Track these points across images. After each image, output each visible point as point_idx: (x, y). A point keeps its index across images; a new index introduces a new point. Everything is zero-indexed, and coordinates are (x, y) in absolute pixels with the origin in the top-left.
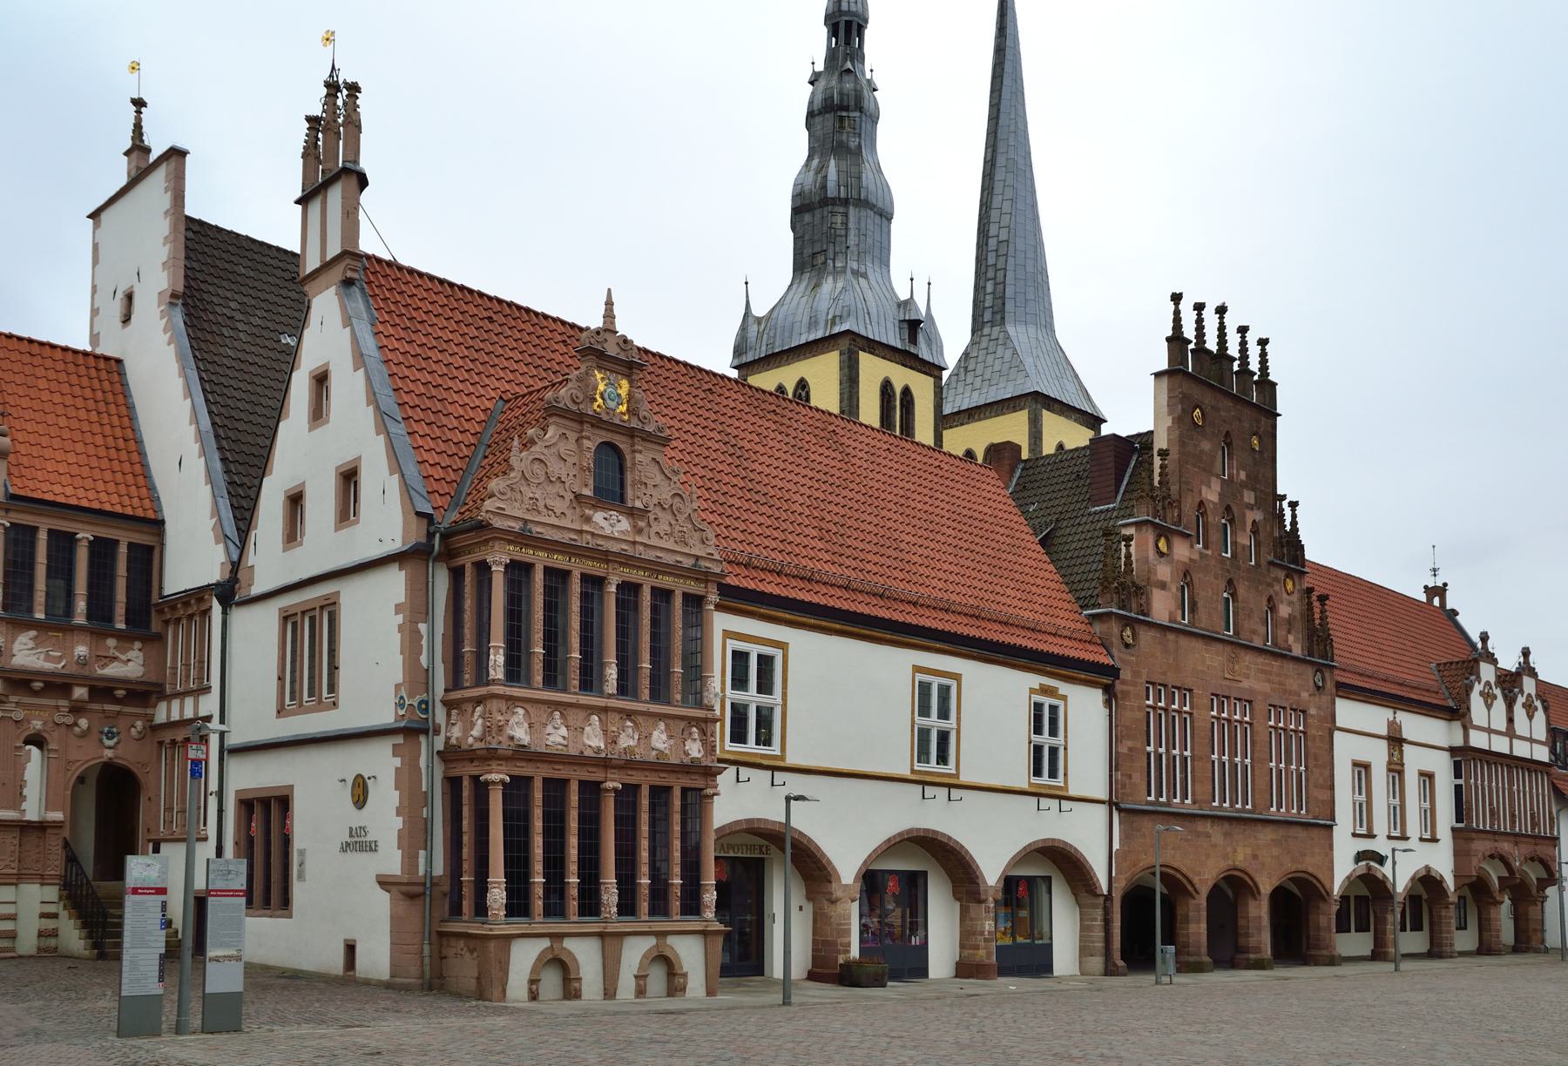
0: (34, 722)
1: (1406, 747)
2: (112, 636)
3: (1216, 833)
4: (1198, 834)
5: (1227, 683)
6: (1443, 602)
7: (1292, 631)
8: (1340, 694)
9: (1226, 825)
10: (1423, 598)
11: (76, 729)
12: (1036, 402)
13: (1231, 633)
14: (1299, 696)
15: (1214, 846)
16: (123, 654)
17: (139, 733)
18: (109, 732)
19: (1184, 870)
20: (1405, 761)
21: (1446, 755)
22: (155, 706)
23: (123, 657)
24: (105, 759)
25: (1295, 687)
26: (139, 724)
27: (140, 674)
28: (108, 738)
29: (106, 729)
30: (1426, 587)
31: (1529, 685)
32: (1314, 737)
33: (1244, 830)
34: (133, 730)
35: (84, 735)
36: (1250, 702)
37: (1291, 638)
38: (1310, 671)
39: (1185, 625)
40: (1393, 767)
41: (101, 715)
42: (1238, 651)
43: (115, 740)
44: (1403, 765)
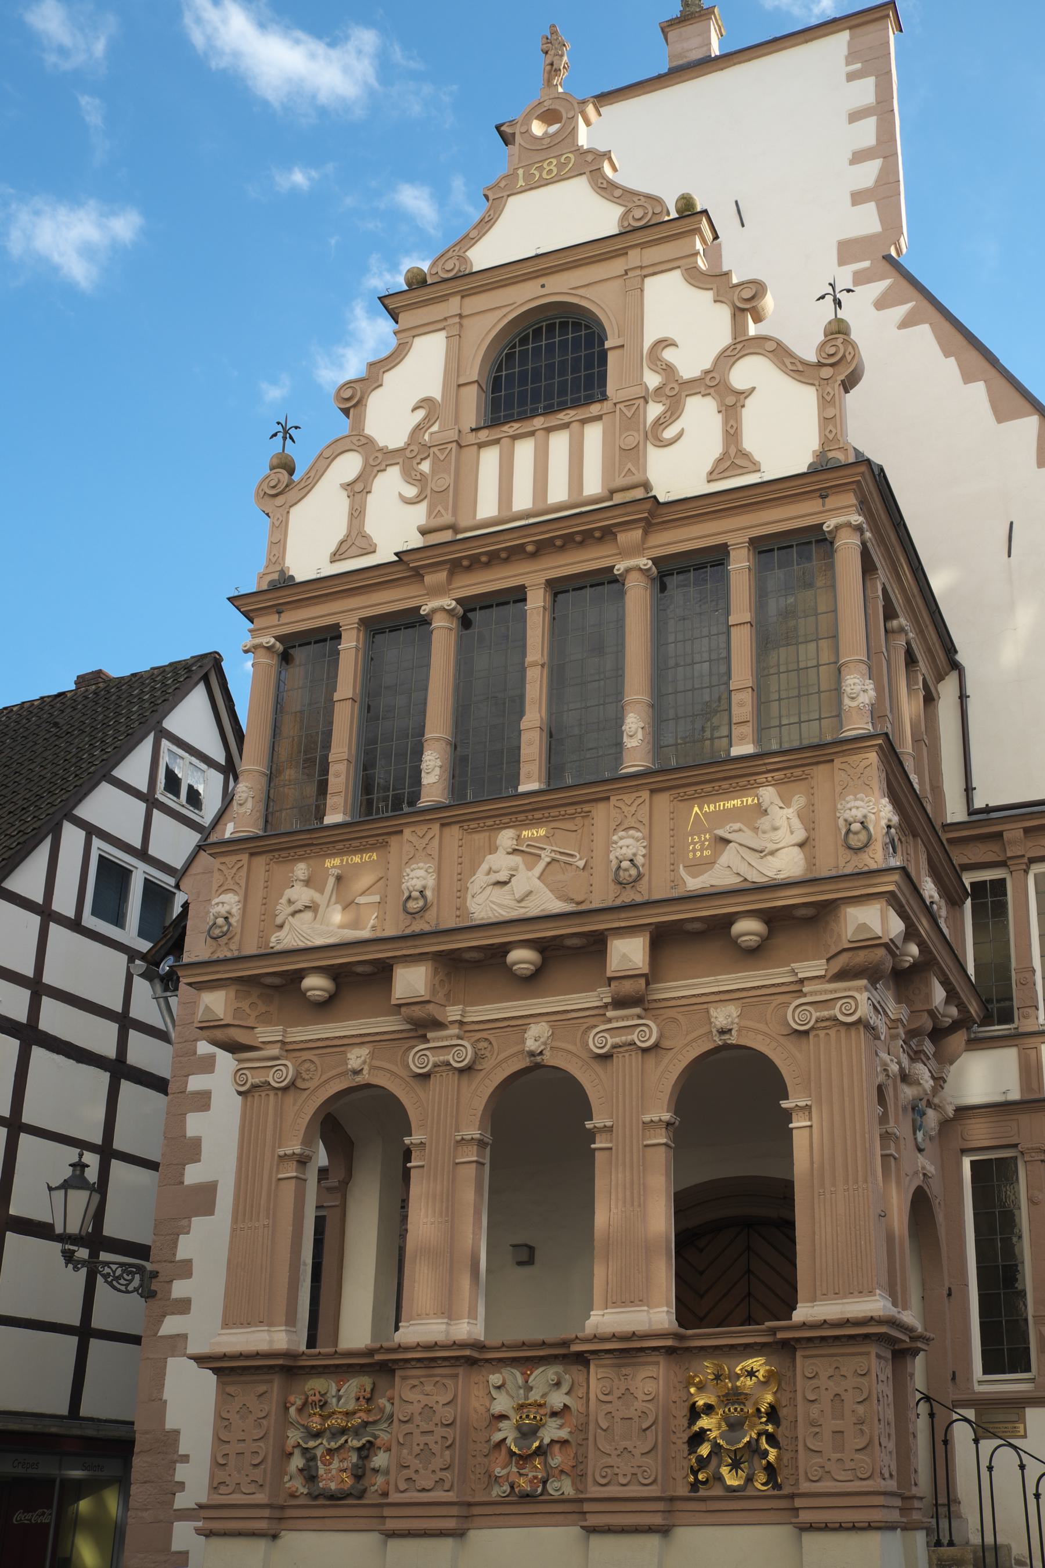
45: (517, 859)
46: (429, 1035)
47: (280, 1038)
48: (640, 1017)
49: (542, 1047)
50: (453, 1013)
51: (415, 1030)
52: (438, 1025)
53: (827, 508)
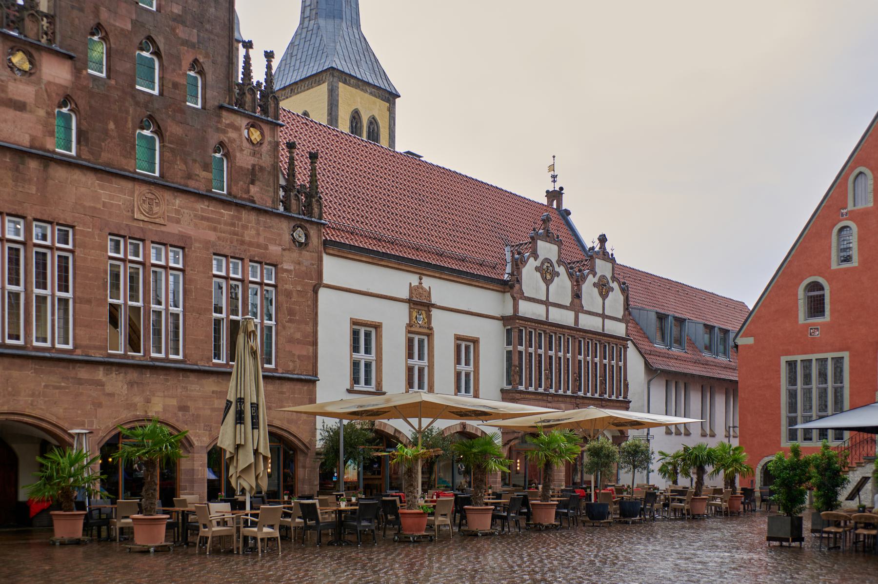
1: (435, 312)
3: (116, 383)
4: (80, 382)
5: (141, 224)
6: (559, 204)
7: (257, 183)
8: (328, 251)
9: (133, 375)
10: (544, 201)
12: (333, 76)
13: (225, 192)
14: (266, 248)
15: (111, 395)
19: (54, 420)
20: (433, 325)
21: (498, 324)
25: (261, 240)
30: (547, 192)
31: (603, 268)
32: (289, 294)
33: (167, 380)
36: (183, 248)
37: (253, 190)
38: (285, 227)
39: (155, 177)
40: (413, 329)
42: (159, 193)
44: (431, 329)
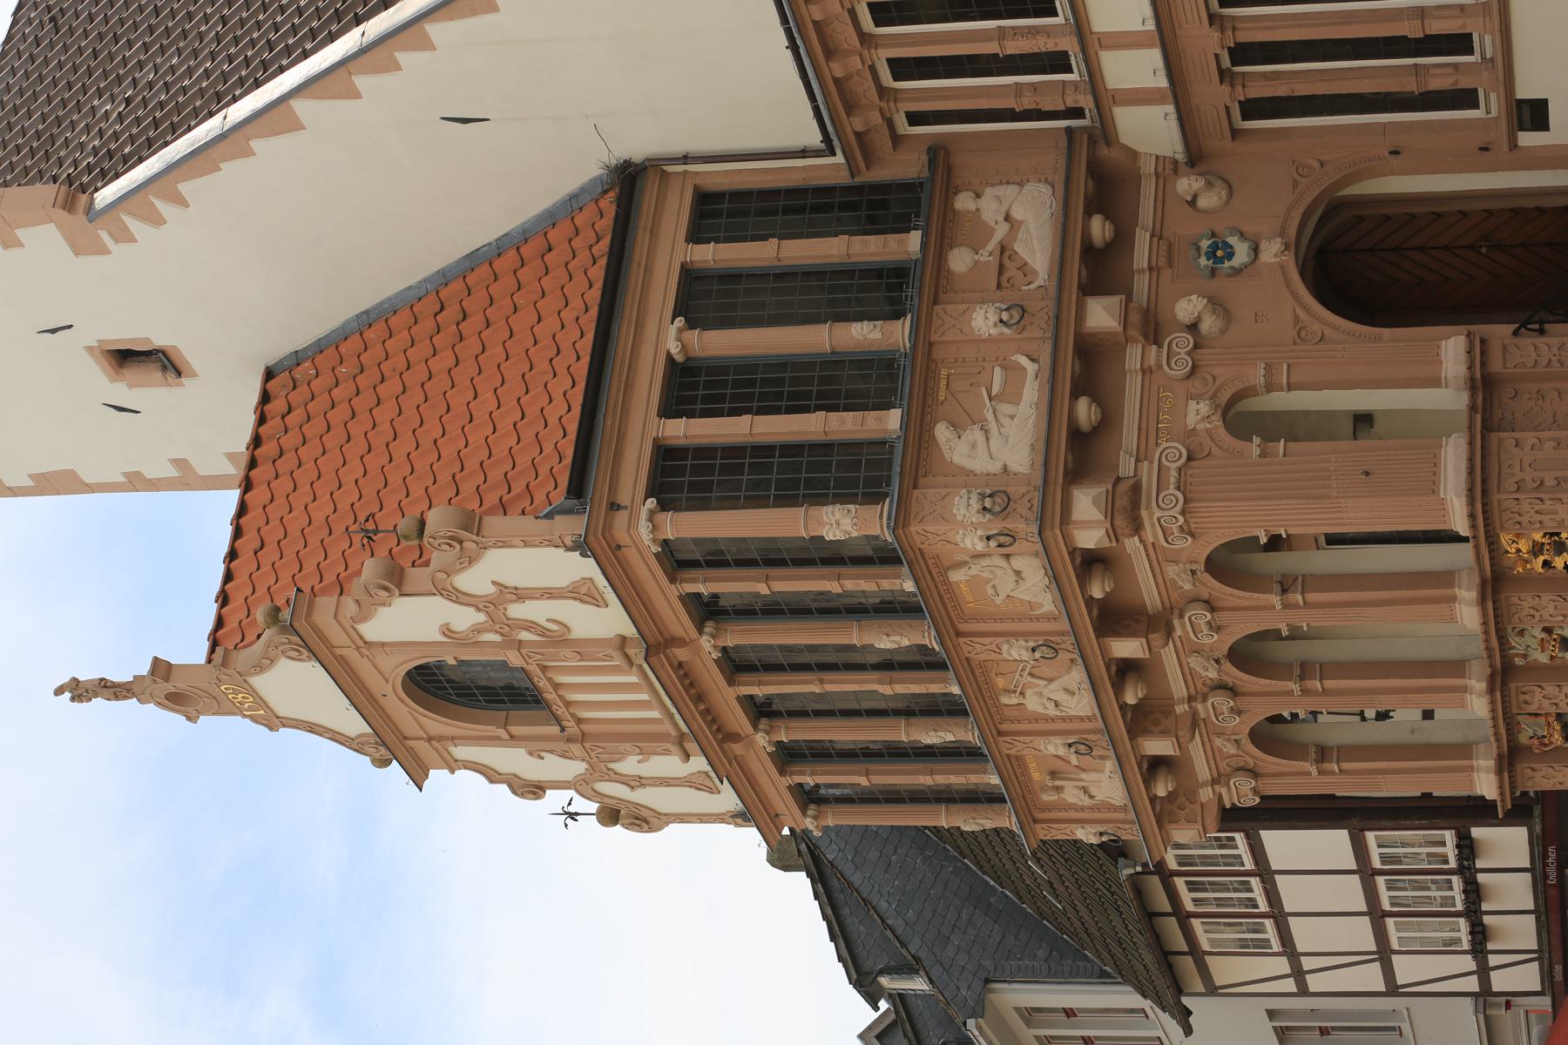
0: (1192, 420)
2: (941, 259)
11: (1208, 325)
16: (991, 231)
17: (1210, 185)
18: (1212, 254)
22: (1134, 155)
23: (1001, 230)
24: (1289, 260)
26: (1186, 185)
27: (1045, 190)
28: (1230, 255)
29: (1203, 261)
34: (1203, 203)
35: (1216, 304)
41: (1166, 274)
43: (1232, 240)
45: (1028, 693)
46: (1203, 716)
47: (1210, 788)
48: (1181, 616)
49: (1213, 662)
50: (1181, 709)
51: (1199, 725)
52: (1194, 715)
53: (631, 543)
